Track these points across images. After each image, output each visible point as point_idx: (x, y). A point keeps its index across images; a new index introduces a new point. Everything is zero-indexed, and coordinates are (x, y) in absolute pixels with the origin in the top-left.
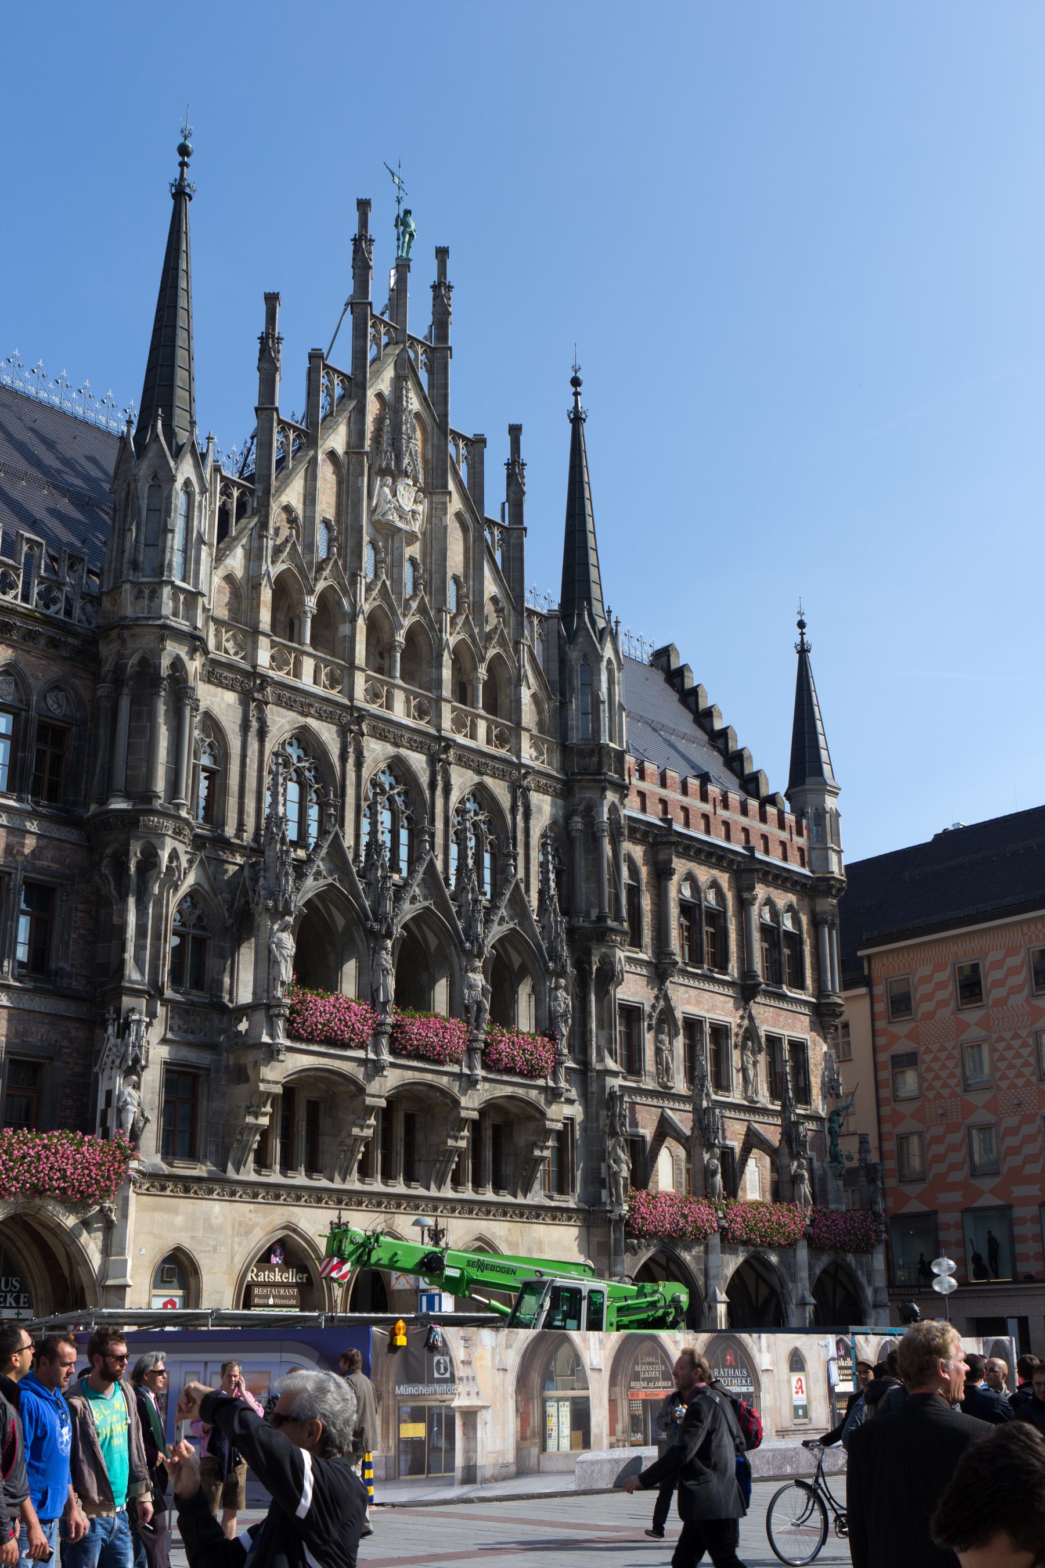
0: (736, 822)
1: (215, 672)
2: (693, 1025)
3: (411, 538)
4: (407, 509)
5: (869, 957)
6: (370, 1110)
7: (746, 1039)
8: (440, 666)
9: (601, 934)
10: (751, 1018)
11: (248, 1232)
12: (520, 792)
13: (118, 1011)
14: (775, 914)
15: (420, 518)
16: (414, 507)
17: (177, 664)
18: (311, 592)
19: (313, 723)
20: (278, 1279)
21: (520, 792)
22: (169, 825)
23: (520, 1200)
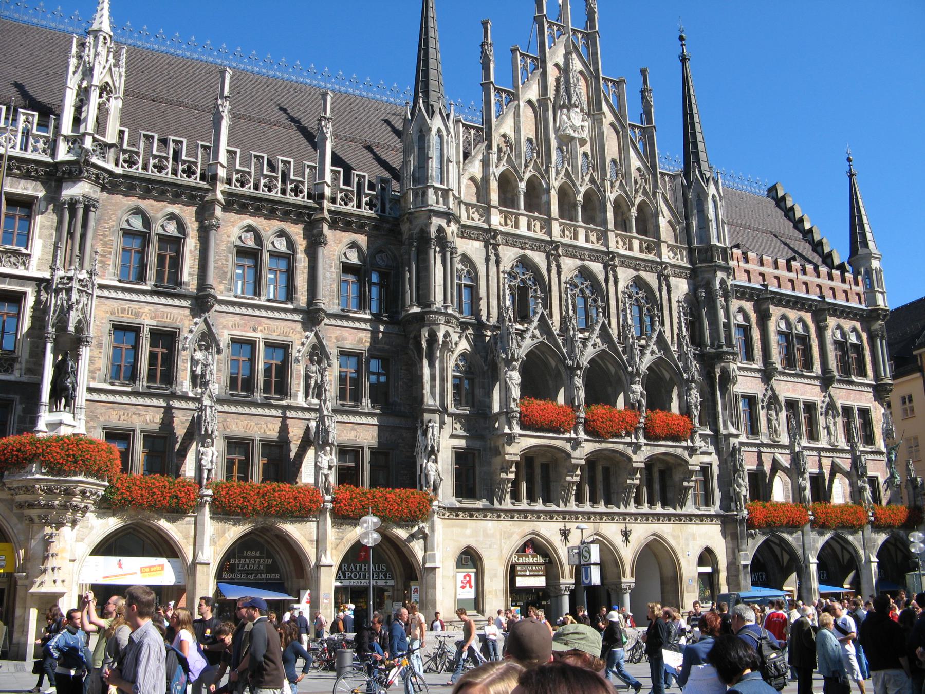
0: (812, 282)
1: (466, 232)
2: (791, 404)
3: (583, 142)
4: (577, 125)
5: (920, 355)
6: (576, 466)
7: (827, 409)
8: (605, 211)
9: (720, 357)
10: (830, 396)
11: (510, 536)
12: (663, 277)
13: (422, 422)
14: (843, 334)
15: (586, 129)
16: (583, 124)
17: (440, 230)
18: (521, 180)
19: (529, 253)
20: (531, 561)
21: (663, 277)
22: (442, 319)
23: (679, 511)
